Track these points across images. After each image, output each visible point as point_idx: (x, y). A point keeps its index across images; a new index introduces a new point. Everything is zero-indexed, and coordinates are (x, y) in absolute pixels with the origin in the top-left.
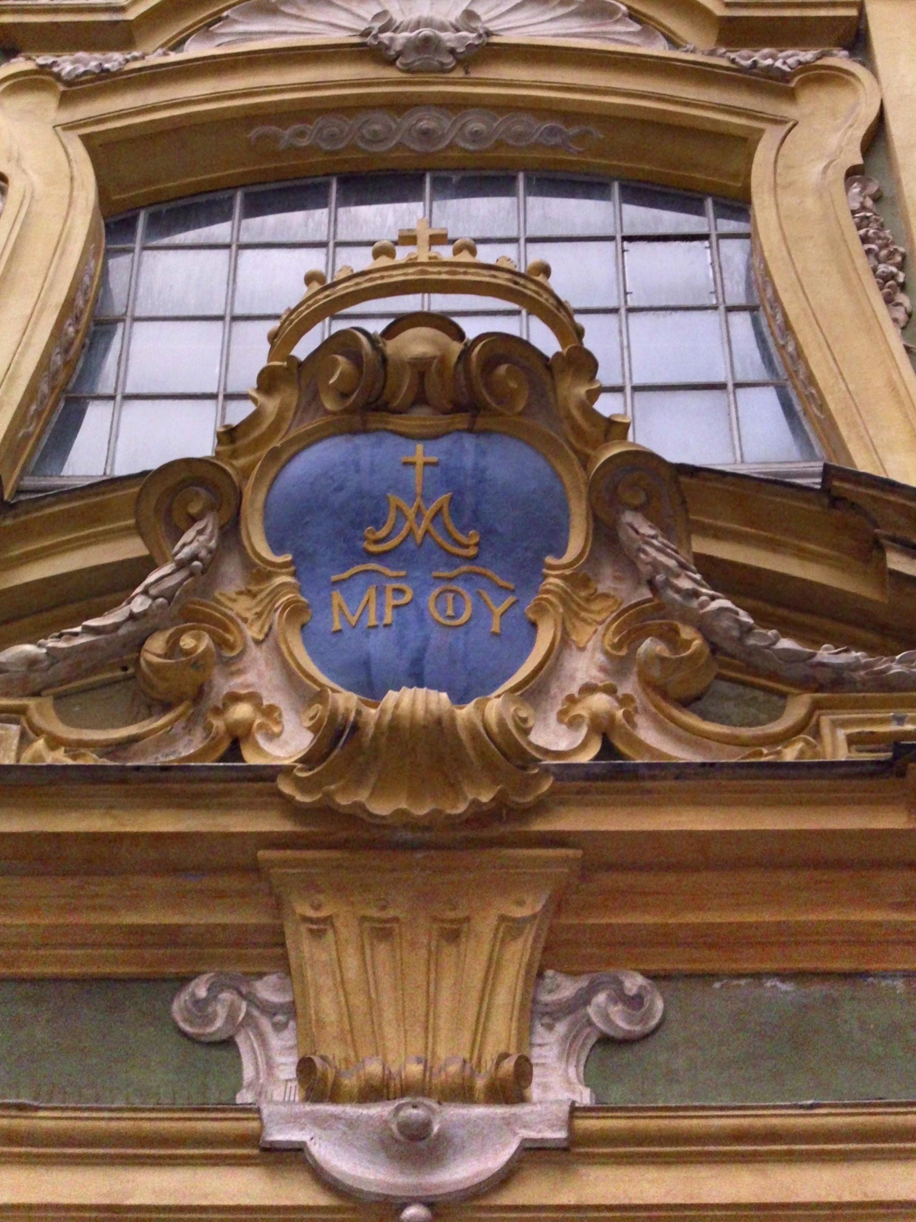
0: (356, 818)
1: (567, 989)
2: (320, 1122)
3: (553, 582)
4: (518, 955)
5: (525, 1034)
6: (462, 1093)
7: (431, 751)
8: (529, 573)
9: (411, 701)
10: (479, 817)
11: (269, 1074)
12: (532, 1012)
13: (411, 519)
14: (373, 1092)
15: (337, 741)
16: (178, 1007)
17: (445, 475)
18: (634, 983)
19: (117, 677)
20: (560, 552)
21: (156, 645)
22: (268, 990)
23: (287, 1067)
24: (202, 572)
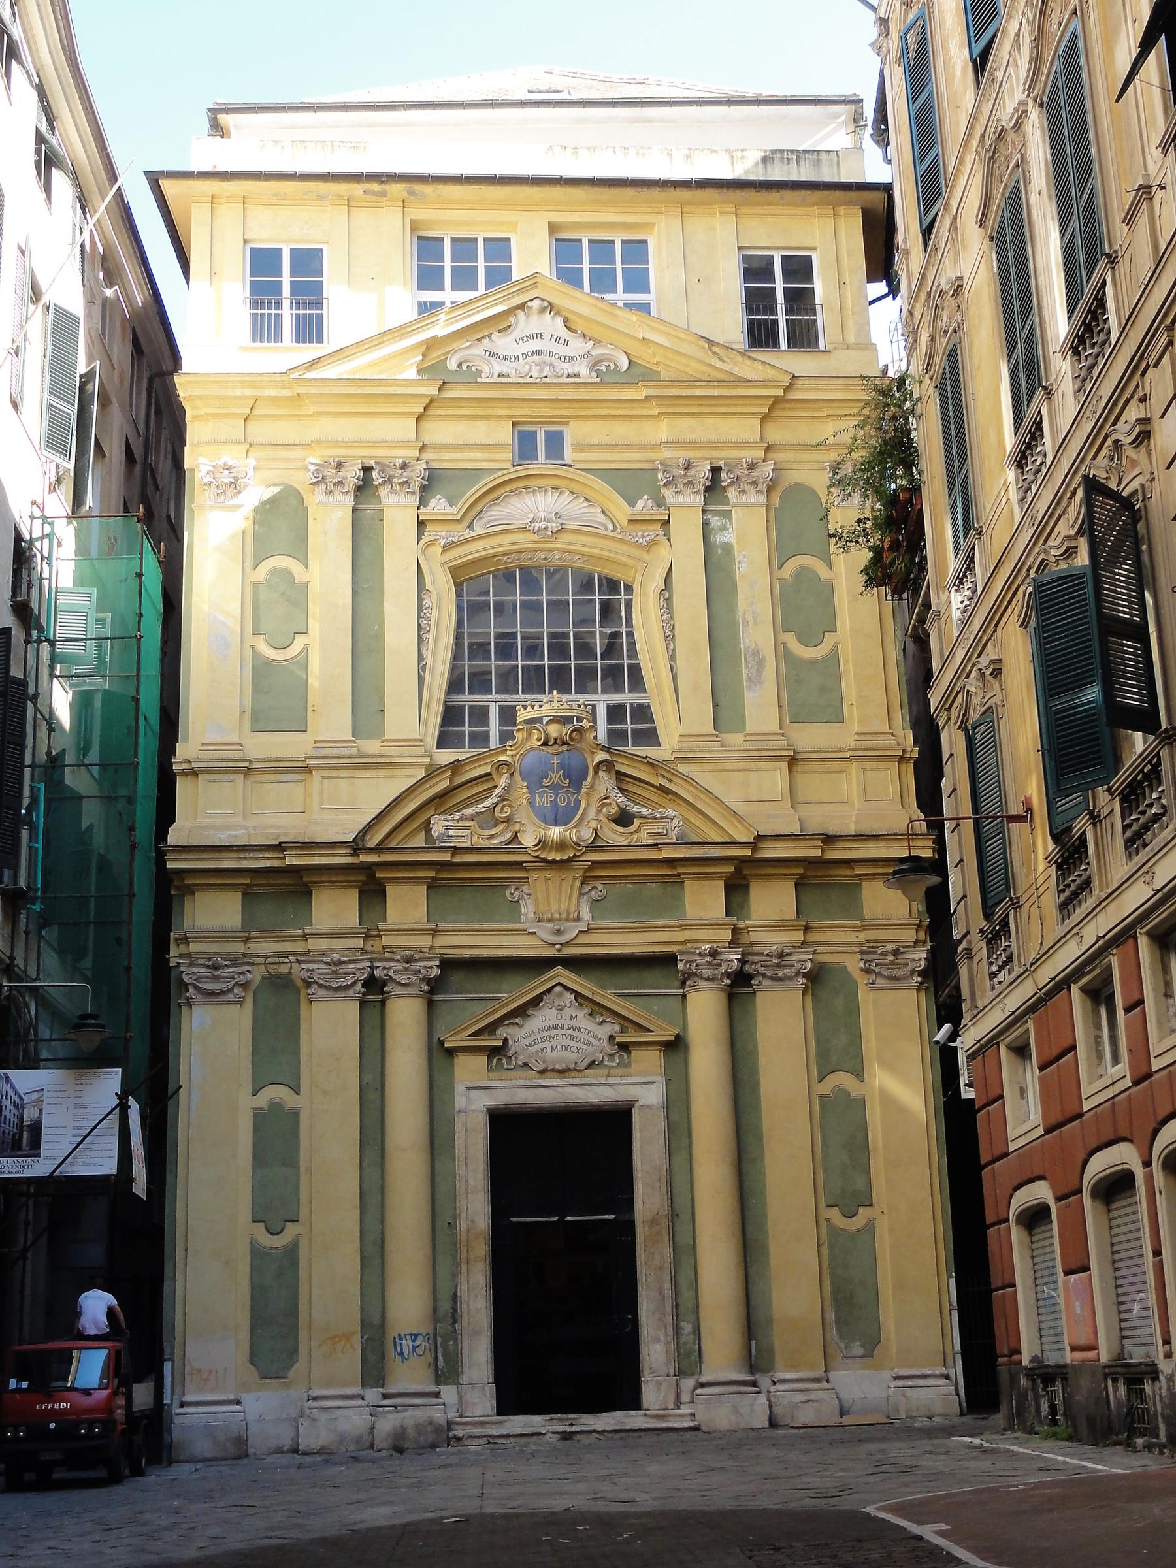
0: (545, 861)
1: (587, 888)
2: (539, 927)
3: (584, 790)
4: (578, 882)
5: (579, 902)
6: (567, 920)
7: (562, 846)
8: (579, 788)
9: (555, 833)
10: (570, 860)
11: (528, 909)
12: (581, 894)
13: (555, 776)
14: (550, 920)
15: (542, 844)
16: (508, 893)
17: (561, 766)
18: (600, 887)
19: (490, 819)
20: (586, 779)
21: (498, 809)
22: (525, 888)
23: (531, 909)
24: (508, 789)
